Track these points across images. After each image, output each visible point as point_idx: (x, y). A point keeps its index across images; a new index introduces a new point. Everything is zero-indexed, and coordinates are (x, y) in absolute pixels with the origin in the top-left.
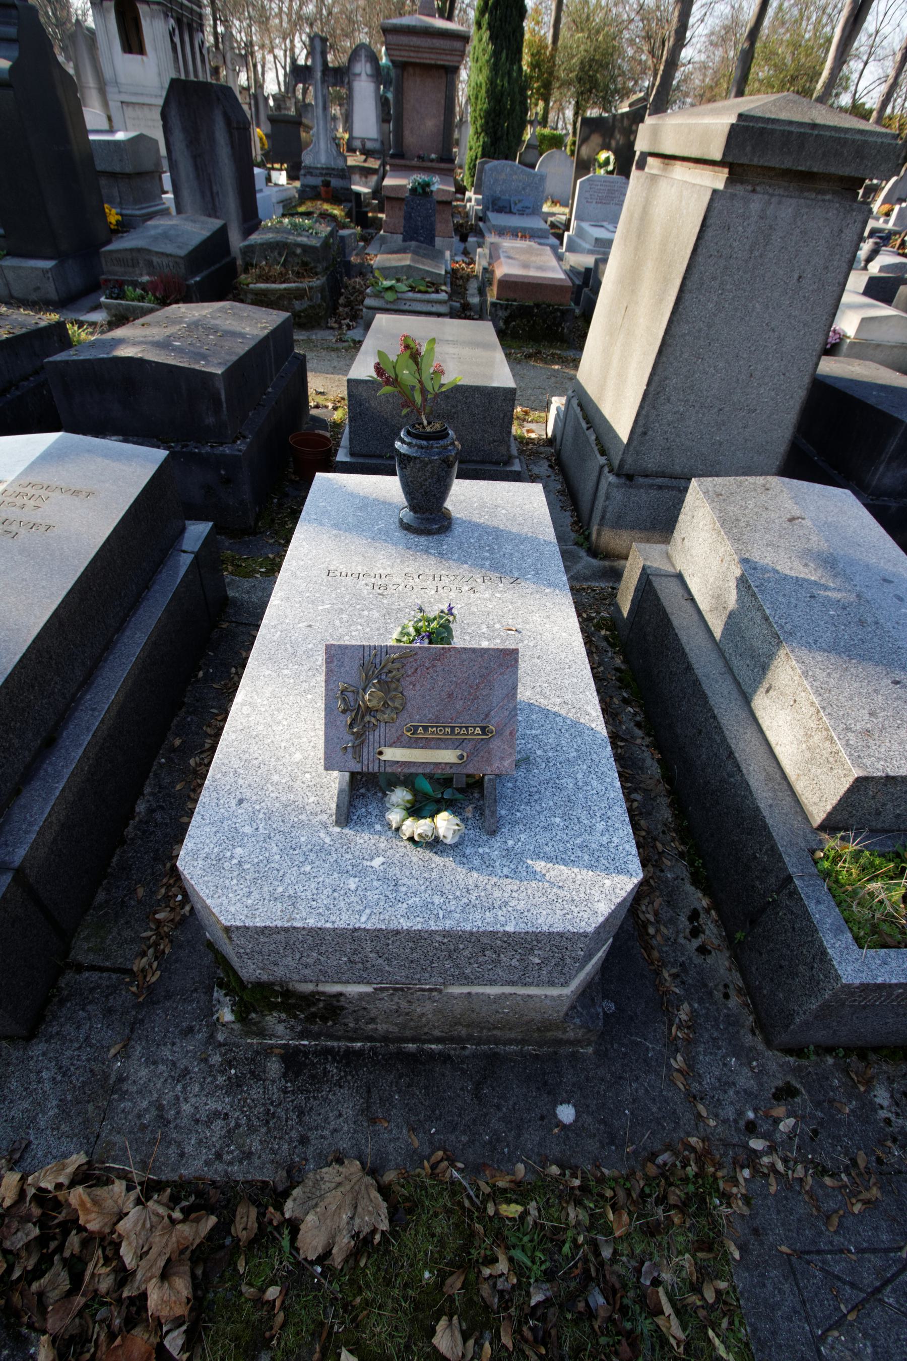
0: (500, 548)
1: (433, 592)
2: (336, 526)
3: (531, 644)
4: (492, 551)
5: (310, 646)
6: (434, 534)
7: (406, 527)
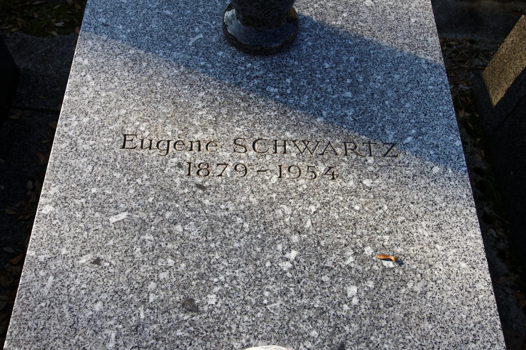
0: (366, 80)
1: (275, 179)
2: (134, 39)
3: (418, 289)
4: (354, 87)
5: (98, 307)
6: (274, 54)
7: (231, 40)
